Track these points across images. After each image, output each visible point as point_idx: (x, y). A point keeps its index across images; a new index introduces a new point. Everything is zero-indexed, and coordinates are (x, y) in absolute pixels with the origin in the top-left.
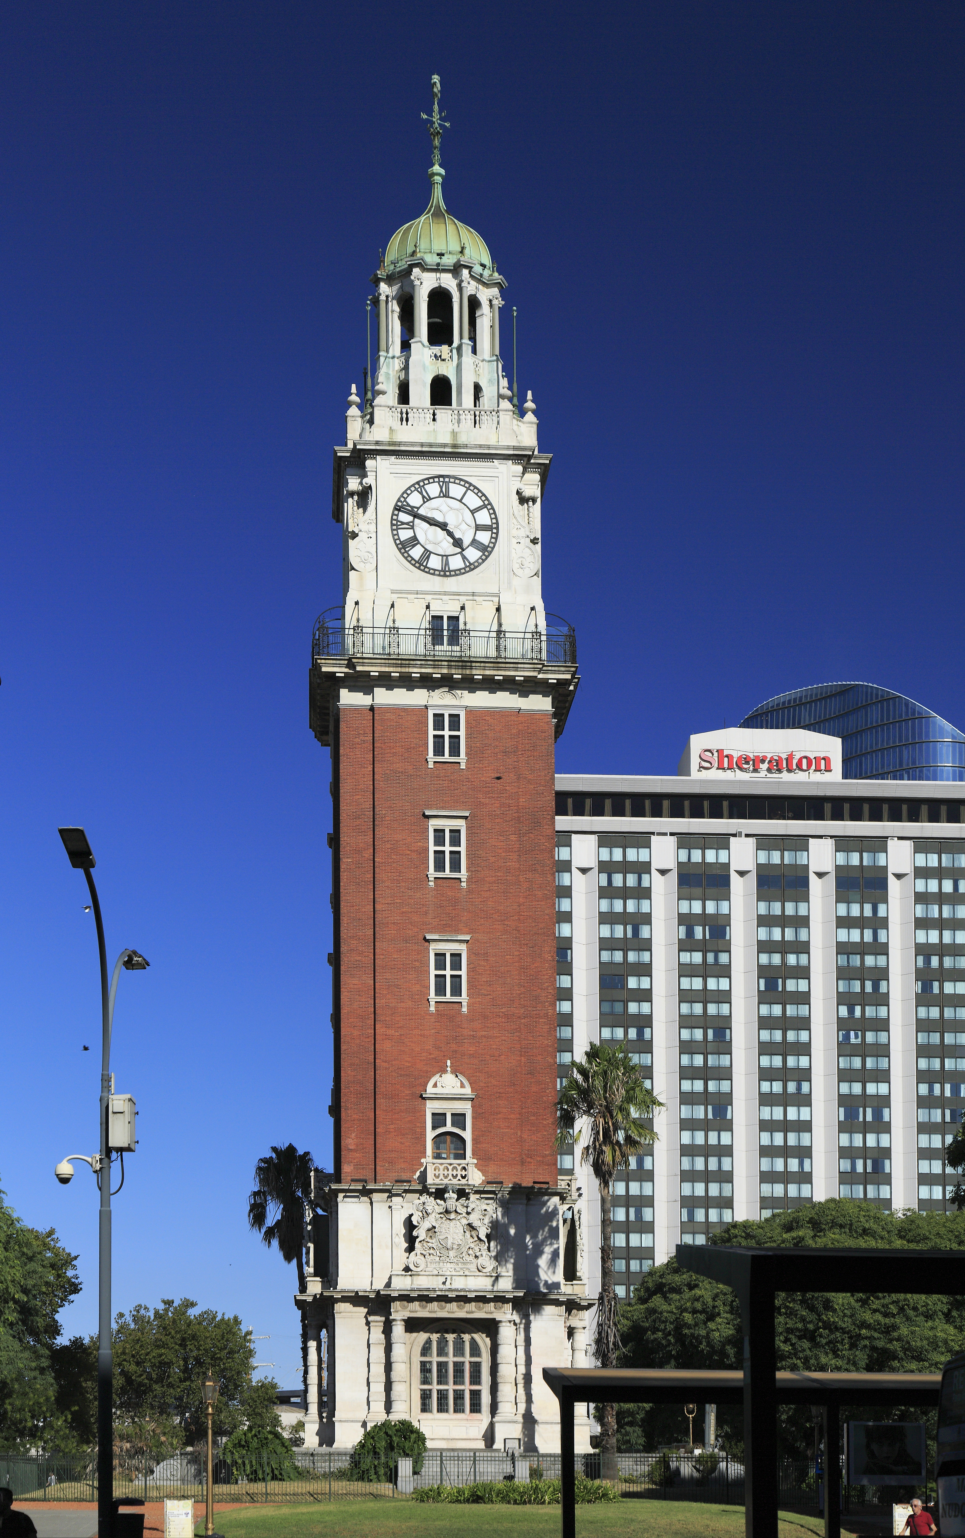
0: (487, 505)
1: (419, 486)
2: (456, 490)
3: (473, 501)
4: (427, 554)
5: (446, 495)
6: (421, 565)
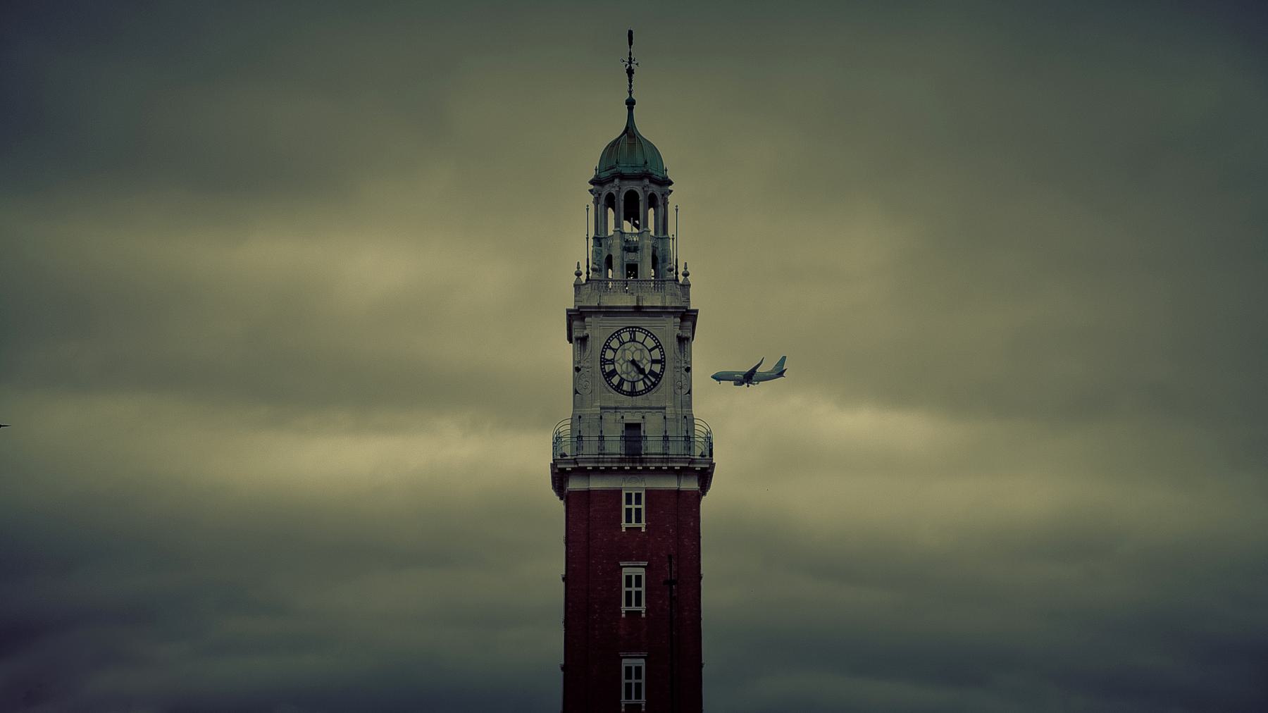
0: (658, 346)
1: (617, 334)
2: (640, 336)
3: (650, 343)
4: (622, 381)
5: (634, 340)
6: (618, 388)
